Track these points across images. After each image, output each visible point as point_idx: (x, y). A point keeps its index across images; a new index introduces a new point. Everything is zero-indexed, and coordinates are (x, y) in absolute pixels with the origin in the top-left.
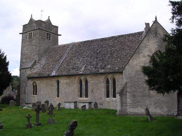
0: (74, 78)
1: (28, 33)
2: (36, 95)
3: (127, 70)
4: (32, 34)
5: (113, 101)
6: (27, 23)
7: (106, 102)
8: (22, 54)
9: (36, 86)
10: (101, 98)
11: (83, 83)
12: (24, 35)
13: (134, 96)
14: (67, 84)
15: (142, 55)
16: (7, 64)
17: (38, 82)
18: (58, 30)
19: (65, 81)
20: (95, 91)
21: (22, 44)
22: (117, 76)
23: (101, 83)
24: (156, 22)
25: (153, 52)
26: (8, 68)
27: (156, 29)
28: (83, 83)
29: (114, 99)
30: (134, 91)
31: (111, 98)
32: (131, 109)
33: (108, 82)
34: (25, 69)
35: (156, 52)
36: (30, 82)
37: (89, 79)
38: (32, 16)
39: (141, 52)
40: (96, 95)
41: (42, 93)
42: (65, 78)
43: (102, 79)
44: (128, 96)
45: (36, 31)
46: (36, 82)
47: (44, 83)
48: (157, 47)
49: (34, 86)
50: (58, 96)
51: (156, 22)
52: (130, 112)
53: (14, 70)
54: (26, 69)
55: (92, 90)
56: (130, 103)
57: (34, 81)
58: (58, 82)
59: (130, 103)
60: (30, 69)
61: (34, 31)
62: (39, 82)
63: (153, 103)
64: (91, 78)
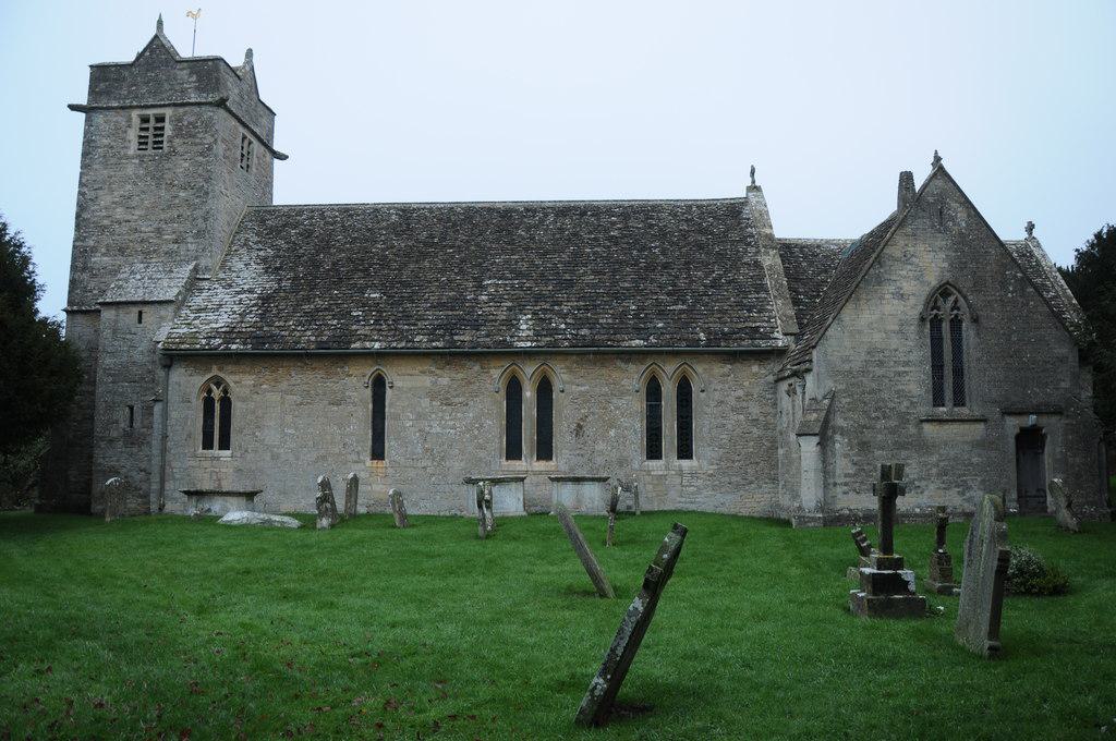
0: (477, 368)
1: (135, 114)
2: (225, 445)
3: (833, 342)
4: (167, 125)
5: (681, 473)
6: (129, 57)
7: (648, 479)
8: (81, 222)
9: (226, 402)
10: (622, 462)
11: (529, 394)
12: (99, 118)
13: (864, 446)
14: (433, 396)
15: (892, 289)
16: (26, 260)
17: (241, 383)
18: (275, 134)
19: (426, 381)
20: (589, 431)
21: (85, 166)
22: (699, 369)
23: (622, 394)
24: (939, 171)
25: (934, 283)
26: (1092, 246)
27: (941, 199)
28: (529, 394)
29: (685, 463)
30: (864, 427)
31: (669, 462)
32: (852, 495)
33: (653, 391)
34: (135, 310)
35: (944, 285)
36: (187, 384)
37: (561, 376)
38: (160, 23)
39: (887, 276)
40: (601, 446)
41: (271, 436)
42: (428, 366)
43: (632, 378)
44: (837, 445)
45: (196, 109)
46: (230, 379)
47: (284, 385)
48: (946, 265)
49: (208, 403)
50: (378, 453)
51: (939, 171)
52: (850, 510)
53: (52, 304)
54: (145, 309)
55: (580, 426)
56: (846, 476)
57: (215, 371)
58: (379, 385)
59: (846, 476)
60: (171, 308)
61: (181, 110)
62: (249, 380)
63: (934, 471)
64: (570, 370)
